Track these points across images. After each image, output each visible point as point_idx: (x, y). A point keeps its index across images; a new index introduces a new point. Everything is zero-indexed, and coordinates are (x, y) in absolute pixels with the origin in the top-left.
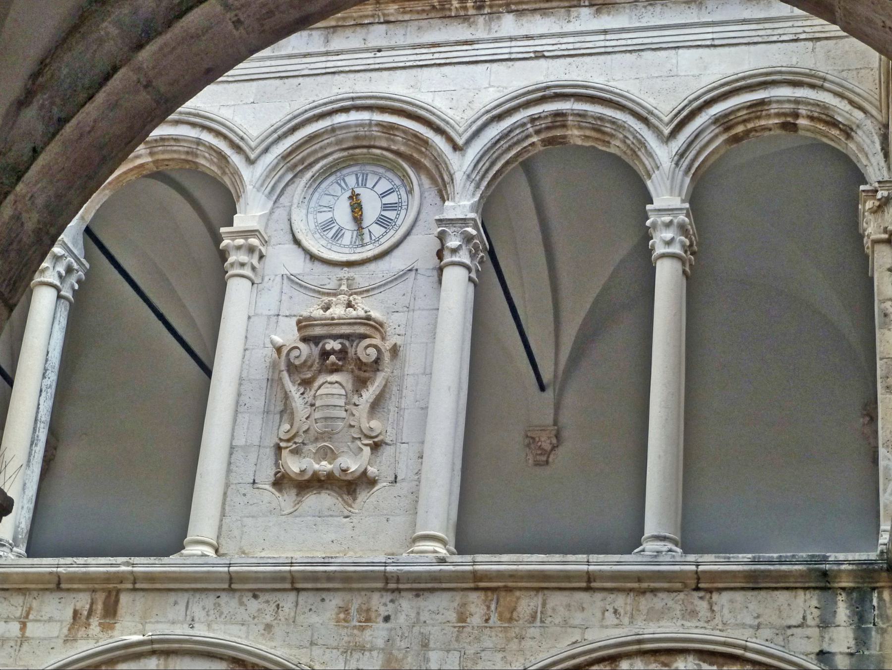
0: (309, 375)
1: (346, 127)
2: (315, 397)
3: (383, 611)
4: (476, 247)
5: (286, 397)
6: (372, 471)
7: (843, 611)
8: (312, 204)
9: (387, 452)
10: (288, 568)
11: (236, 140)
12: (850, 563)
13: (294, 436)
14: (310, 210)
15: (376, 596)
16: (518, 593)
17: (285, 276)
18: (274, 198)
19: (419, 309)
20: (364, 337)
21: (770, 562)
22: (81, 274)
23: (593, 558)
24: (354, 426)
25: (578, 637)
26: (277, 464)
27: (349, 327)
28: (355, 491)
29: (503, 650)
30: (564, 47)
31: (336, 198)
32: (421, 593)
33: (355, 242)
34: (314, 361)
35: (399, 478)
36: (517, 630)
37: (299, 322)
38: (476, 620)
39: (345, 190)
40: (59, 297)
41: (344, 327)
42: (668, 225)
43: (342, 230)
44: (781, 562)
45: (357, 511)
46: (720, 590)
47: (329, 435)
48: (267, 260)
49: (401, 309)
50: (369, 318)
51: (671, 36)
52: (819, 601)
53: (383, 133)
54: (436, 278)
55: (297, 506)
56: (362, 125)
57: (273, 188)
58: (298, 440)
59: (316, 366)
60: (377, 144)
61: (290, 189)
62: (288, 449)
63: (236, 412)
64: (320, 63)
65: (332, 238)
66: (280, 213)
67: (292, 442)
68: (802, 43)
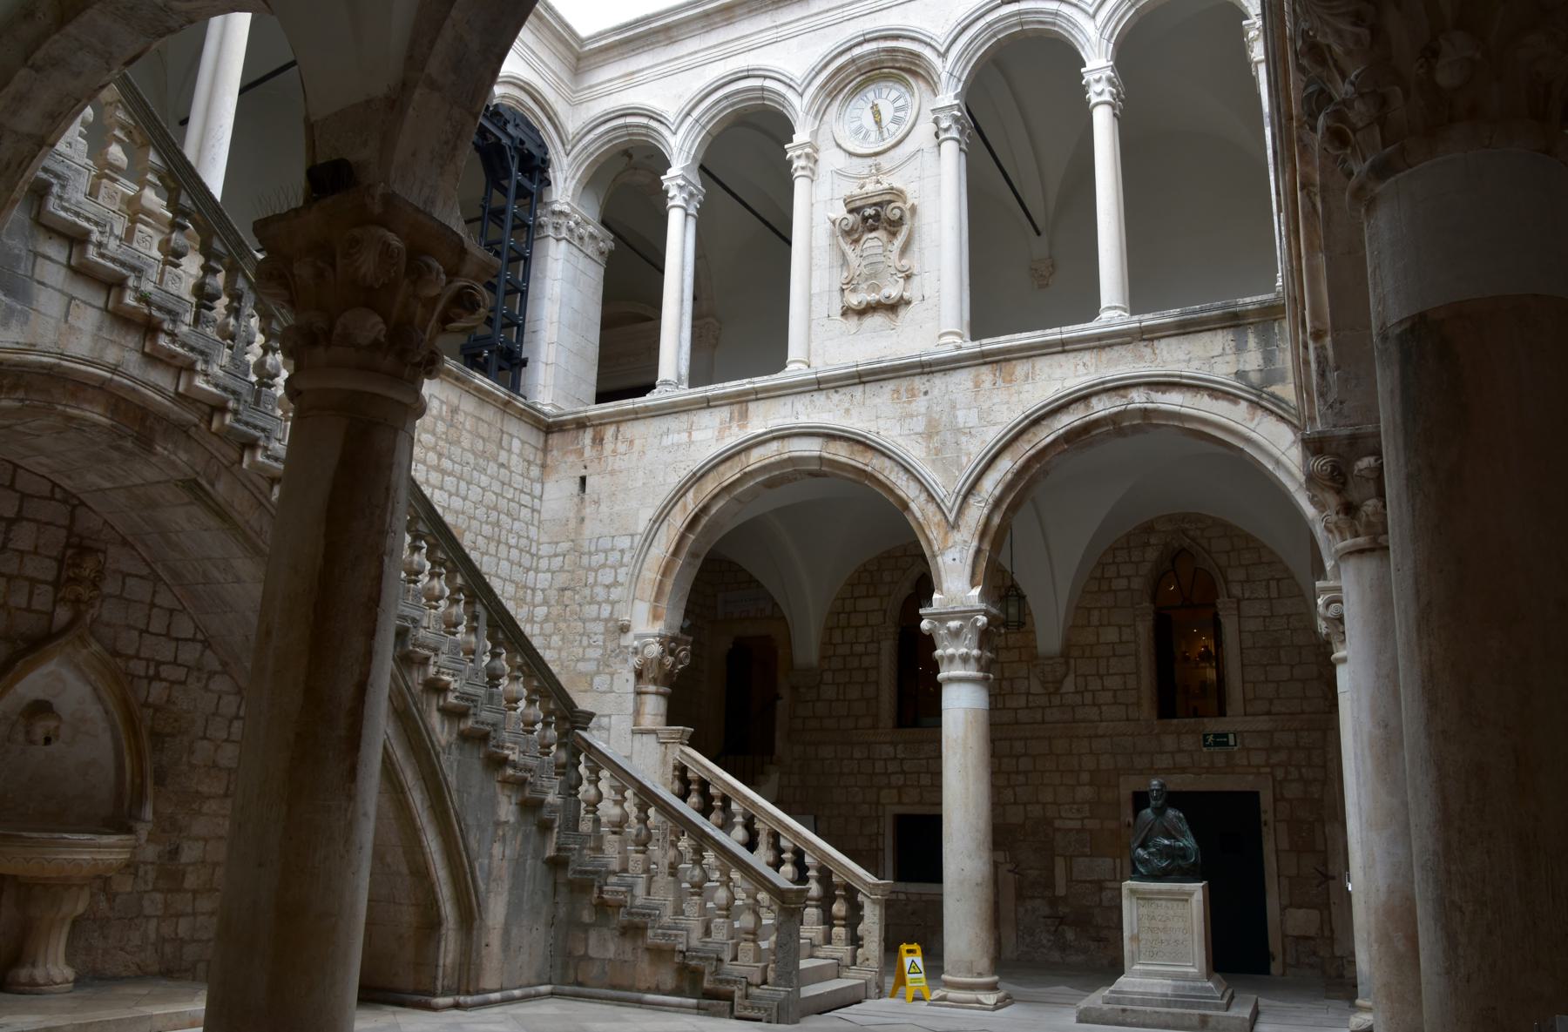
0: (856, 236)
1: (861, 57)
2: (862, 250)
3: (923, 388)
4: (962, 125)
5: (844, 255)
6: (906, 295)
7: (1252, 341)
9: (916, 281)
10: (855, 369)
11: (788, 81)
12: (1254, 303)
13: (851, 280)
15: (917, 379)
16: (1014, 362)
20: (890, 202)
21: (1194, 312)
22: (701, 197)
23: (1064, 329)
25: (1059, 386)
26: (842, 301)
29: (1008, 403)
36: (1016, 387)
37: (845, 200)
38: (987, 385)
40: (687, 215)
42: (1098, 81)
44: (1202, 311)
46: (1159, 338)
47: (874, 275)
48: (820, 163)
50: (892, 189)
52: (1234, 335)
54: (937, 153)
56: (873, 53)
57: (818, 112)
59: (860, 229)
60: (885, 65)
61: (829, 110)
63: (810, 270)
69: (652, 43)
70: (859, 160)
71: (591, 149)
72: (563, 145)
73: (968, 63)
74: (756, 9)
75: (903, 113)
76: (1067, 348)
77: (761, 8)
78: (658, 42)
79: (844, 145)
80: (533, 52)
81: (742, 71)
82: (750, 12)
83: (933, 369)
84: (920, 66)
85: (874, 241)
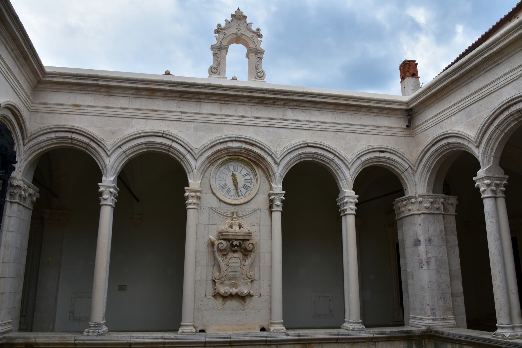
1: (231, 148)
6: (252, 292)
8: (217, 177)
9: (256, 283)
14: (216, 179)
16: (313, 345)
17: (210, 208)
18: (203, 174)
19: (263, 225)
20: (248, 240)
24: (244, 274)
27: (243, 236)
28: (245, 299)
30: (311, 126)
31: (226, 175)
32: (278, 346)
33: (235, 195)
34: (228, 248)
35: (261, 295)
39: (229, 172)
41: (241, 236)
43: (226, 186)
45: (247, 308)
46: (378, 342)
47: (234, 278)
49: (256, 225)
51: (347, 128)
53: (245, 152)
55: (223, 307)
58: (223, 279)
60: (242, 155)
61: (209, 170)
62: (219, 283)
64: (219, 119)
65: (226, 192)
66: (206, 180)
67: (220, 280)
68: (389, 136)
69: (95, 91)
70: (225, 205)
71: (42, 145)
72: (23, 139)
73: (287, 169)
74: (169, 97)
75: (250, 183)
76: (339, 341)
77: (172, 97)
78: (100, 92)
79: (217, 194)
80: (18, 82)
81: (159, 133)
82: (164, 97)
83: (272, 343)
84: (262, 163)
85: (235, 258)
